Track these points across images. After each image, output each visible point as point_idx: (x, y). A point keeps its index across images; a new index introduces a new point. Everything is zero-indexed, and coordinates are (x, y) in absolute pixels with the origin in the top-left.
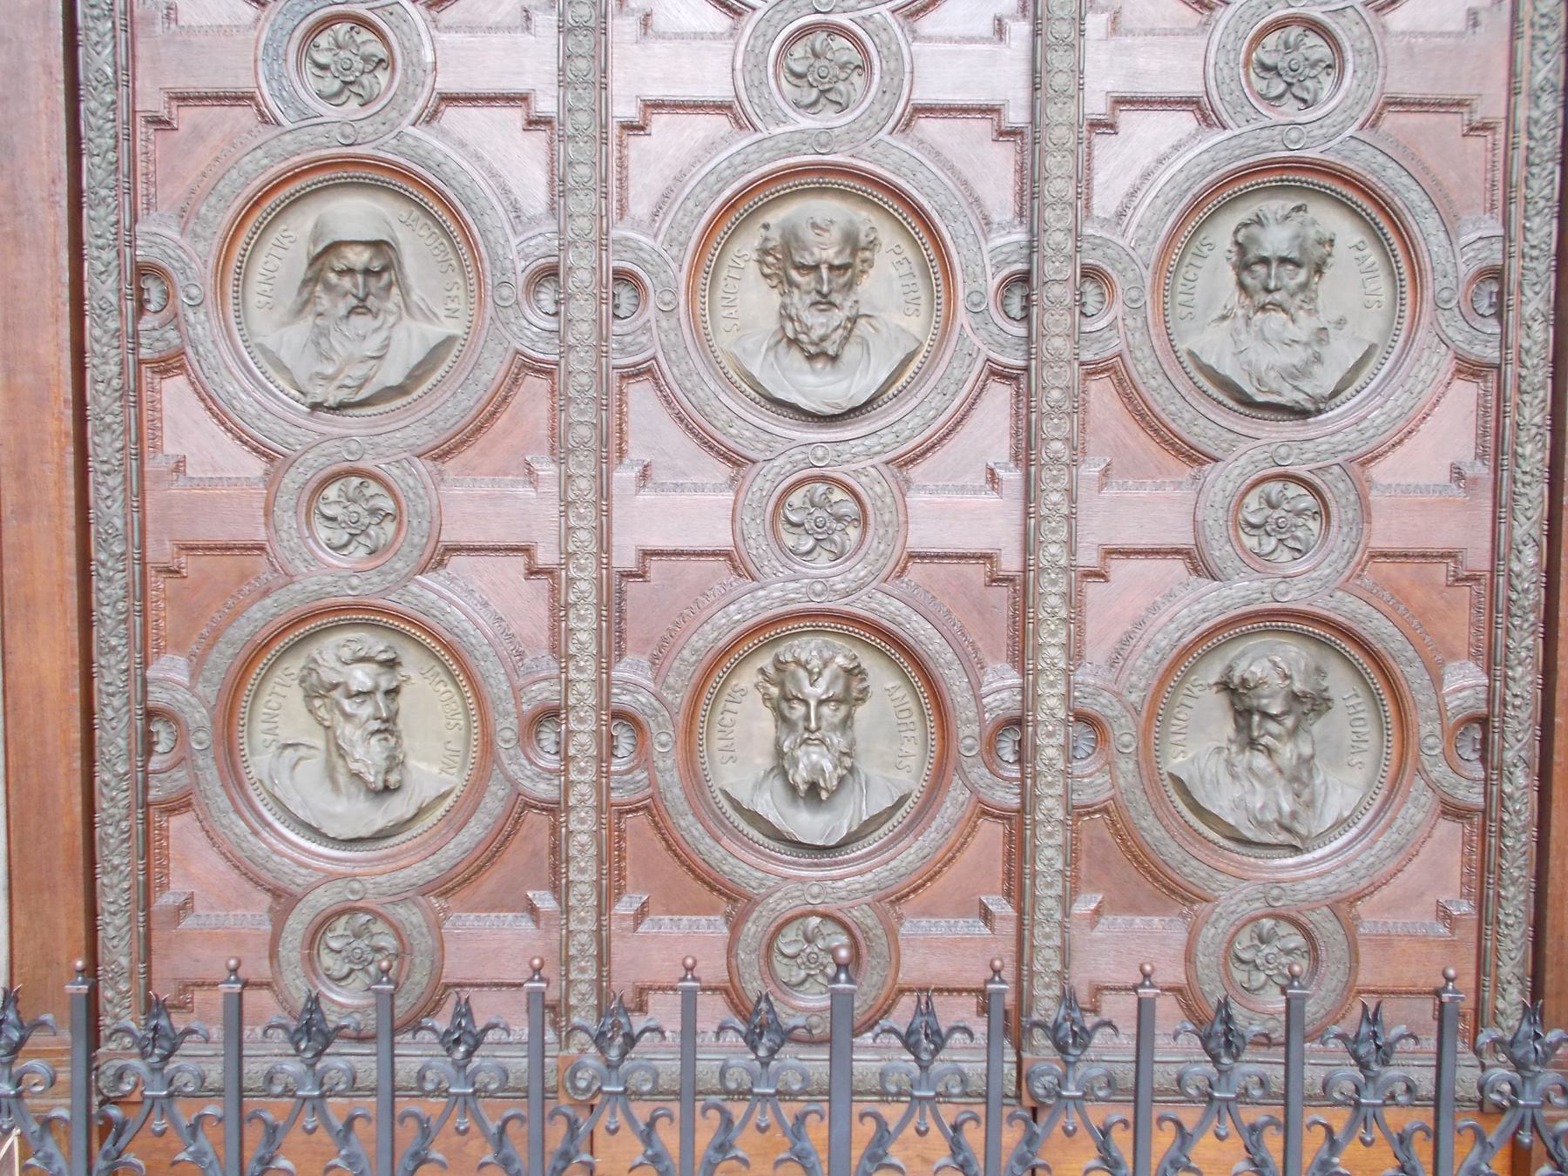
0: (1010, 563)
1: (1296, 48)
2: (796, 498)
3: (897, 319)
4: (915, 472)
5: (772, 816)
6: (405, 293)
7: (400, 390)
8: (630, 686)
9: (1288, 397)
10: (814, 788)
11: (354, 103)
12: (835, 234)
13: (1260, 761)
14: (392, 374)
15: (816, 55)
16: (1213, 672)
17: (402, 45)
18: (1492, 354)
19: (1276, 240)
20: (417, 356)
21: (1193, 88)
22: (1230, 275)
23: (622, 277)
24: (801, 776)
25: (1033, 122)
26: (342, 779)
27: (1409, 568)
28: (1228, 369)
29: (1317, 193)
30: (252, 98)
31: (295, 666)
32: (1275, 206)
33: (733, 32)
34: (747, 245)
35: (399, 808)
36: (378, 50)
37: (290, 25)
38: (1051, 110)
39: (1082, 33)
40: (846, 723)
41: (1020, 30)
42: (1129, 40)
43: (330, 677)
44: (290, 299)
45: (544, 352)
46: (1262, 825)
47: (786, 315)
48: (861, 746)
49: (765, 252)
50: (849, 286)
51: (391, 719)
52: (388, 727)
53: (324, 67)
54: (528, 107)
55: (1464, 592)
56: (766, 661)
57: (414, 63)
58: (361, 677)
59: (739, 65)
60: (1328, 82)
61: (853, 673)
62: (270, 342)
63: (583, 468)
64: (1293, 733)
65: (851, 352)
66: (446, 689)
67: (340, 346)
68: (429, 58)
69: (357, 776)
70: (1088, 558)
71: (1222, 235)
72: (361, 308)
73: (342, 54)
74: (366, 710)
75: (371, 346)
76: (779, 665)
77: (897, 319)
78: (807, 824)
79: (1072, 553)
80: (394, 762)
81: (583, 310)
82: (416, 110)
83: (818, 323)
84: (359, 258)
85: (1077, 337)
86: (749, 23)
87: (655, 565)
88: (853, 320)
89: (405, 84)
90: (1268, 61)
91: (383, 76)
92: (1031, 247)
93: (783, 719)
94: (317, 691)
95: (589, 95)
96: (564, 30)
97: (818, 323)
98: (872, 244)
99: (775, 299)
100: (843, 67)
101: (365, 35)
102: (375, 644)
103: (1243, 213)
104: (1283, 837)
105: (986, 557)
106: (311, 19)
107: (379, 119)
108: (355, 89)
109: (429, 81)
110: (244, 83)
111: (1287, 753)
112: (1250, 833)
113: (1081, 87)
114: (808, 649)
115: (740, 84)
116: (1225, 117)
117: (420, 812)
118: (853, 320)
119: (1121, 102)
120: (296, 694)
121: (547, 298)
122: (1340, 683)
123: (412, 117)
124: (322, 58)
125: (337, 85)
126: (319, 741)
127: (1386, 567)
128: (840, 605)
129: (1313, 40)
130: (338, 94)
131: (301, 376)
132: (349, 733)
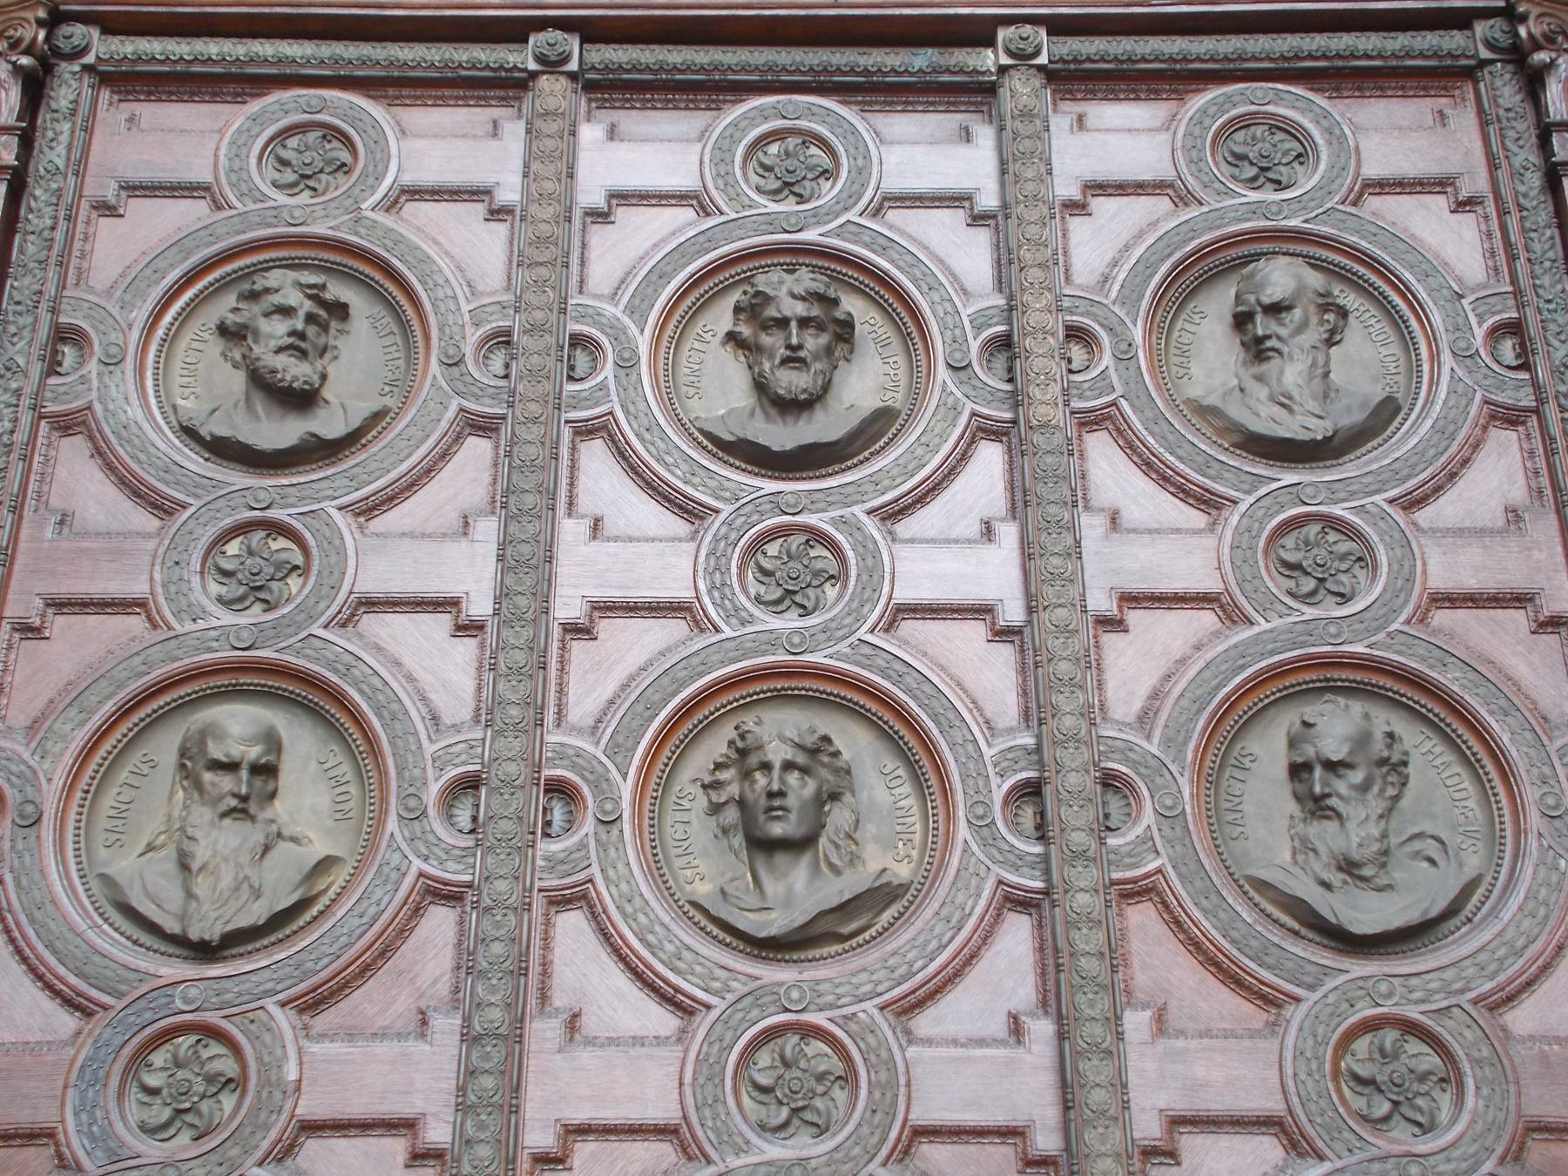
1: (1396, 1056)
11: (185, 1138)
15: (787, 1064)
17: (259, 1059)
25: (1067, 1148)
30: (51, 1134)
33: (682, 1036)
36: (228, 1066)
37: (119, 1040)
38: (1090, 1136)
39: (1120, 1036)
41: (1042, 1029)
42: (1180, 1043)
53: (154, 1092)
54: (415, 1136)
57: (271, 1079)
59: (688, 1078)
60: (1445, 1100)
68: (291, 1073)
73: (180, 1074)
82: (265, 1145)
86: (703, 1024)
89: (255, 1110)
90: (1363, 1071)
91: (228, 1101)
95: (493, 1122)
96: (469, 1038)
100: (820, 1077)
101: (215, 1048)
106: (148, 1031)
107: (214, 1158)
108: (189, 1118)
109: (288, 1106)
110: (44, 1115)
113: (1126, 1105)
115: (690, 1101)
116: (1320, 1144)
119: (1178, 1122)
123: (259, 1154)
124: (152, 1081)
125: (166, 1114)
129: (1414, 1046)
130: (165, 1126)
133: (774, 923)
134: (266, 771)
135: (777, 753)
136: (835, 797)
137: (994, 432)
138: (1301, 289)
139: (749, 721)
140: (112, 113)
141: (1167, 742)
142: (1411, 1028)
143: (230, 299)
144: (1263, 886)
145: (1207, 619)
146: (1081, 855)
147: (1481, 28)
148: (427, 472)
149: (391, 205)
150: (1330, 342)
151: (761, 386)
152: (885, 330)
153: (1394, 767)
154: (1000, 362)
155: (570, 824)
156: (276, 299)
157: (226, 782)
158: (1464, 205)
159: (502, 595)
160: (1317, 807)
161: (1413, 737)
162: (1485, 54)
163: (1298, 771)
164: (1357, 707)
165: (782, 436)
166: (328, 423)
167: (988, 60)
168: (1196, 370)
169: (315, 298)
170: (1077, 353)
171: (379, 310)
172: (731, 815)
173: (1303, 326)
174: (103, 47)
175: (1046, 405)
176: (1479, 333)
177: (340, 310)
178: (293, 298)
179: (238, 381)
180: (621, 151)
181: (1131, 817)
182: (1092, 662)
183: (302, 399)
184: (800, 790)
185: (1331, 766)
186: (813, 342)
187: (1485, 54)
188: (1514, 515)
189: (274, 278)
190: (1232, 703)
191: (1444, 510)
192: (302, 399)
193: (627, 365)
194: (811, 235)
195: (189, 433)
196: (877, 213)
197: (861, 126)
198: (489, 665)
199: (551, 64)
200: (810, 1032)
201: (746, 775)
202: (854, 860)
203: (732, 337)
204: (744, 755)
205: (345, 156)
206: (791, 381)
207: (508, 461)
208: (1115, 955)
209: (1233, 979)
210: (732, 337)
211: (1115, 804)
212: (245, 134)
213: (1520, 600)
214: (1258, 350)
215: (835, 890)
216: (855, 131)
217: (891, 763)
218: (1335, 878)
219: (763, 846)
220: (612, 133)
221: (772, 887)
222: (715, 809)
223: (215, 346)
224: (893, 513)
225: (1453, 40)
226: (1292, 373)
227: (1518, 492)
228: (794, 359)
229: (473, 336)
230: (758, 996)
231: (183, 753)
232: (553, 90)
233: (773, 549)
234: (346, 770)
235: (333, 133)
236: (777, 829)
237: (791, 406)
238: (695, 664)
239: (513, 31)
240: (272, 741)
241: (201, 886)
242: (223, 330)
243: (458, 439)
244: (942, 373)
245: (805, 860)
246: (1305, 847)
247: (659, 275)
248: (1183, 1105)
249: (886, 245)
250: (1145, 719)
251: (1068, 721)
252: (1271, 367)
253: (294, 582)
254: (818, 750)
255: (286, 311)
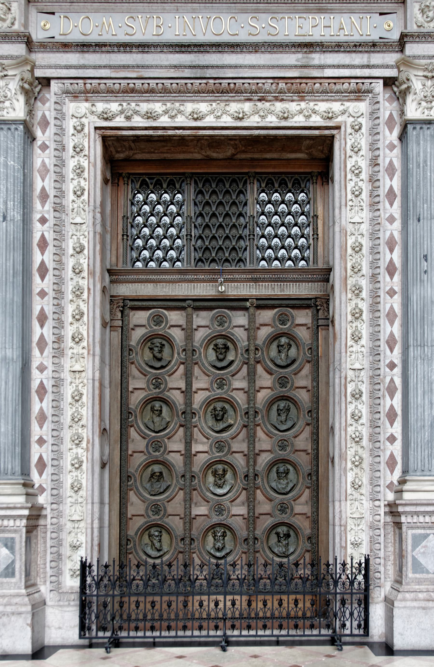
0: (246, 516)
2: (217, 507)
3: (230, 481)
4: (233, 503)
5: (213, 553)
6: (163, 478)
7: (163, 492)
8: (193, 535)
9: (283, 491)
10: (218, 548)
12: (221, 470)
13: (281, 544)
14: (162, 490)
16: (274, 531)
18: (310, 485)
19: (281, 470)
20: (165, 488)
21: (270, 449)
22: (276, 475)
23: (193, 476)
24: (217, 547)
26: (154, 548)
27: (301, 516)
28: (275, 488)
29: (287, 463)
31: (147, 532)
32: (281, 465)
33: (208, 442)
34: (210, 471)
35: (161, 553)
36: (160, 445)
40: (224, 539)
43: (152, 533)
44: (148, 480)
45: (183, 487)
46: (281, 553)
47: (215, 481)
48: (226, 543)
49: (212, 472)
50: (224, 477)
51: (160, 540)
52: (160, 541)
55: (308, 519)
56: (212, 531)
58: (157, 534)
61: (225, 532)
62: (145, 486)
63: (188, 503)
64: (285, 539)
65: (224, 486)
66: (168, 535)
67: (155, 486)
69: (156, 548)
70: (256, 515)
71: (275, 469)
72: (158, 481)
74: (157, 538)
75: (159, 486)
76: (214, 531)
77: (230, 481)
78: (218, 554)
79: (254, 514)
80: (161, 546)
81: (188, 481)
83: (219, 482)
84: (158, 474)
85: (254, 484)
86: (210, 441)
87: (197, 517)
88: (224, 482)
92: (248, 471)
93: (215, 539)
94: (150, 536)
96: (186, 443)
97: (219, 482)
98: (227, 471)
99: (214, 479)
102: (159, 529)
103: (276, 467)
104: (284, 555)
105: (242, 515)
111: (284, 542)
112: (279, 554)
114: (218, 529)
117: (165, 553)
118: (224, 482)
120: (147, 537)
121: (183, 479)
122: (292, 533)
126: (150, 543)
127: (297, 516)
128: (222, 522)
129: (285, 442)
131: (149, 490)
132: (155, 542)
133: (218, 429)
134: (161, 411)
135: (219, 409)
136: (225, 413)
137: (246, 363)
138: (285, 342)
139: (215, 404)
140: (132, 313)
141: (263, 407)
142: (285, 440)
143: (149, 344)
144: (272, 424)
145: (270, 390)
146: (252, 422)
147: (313, 300)
148: (176, 370)
149: (169, 328)
150: (288, 350)
151: (217, 357)
152: (233, 347)
153: (288, 410)
154: (247, 353)
155: (195, 417)
156: (156, 345)
157: (157, 412)
158: (308, 328)
159: (186, 389)
160: (279, 415)
161: (292, 406)
162: (313, 305)
163: (278, 410)
164: (285, 402)
165: (220, 365)
166: (163, 363)
167: (248, 304)
168: (272, 353)
169: (161, 344)
170: (257, 352)
171: (168, 344)
172: (213, 416)
173: (285, 348)
174: (130, 304)
175: (252, 362)
176: (306, 349)
177: (164, 345)
178: (158, 345)
179: (151, 355)
180: (199, 320)
181: (258, 416)
182: (255, 397)
183: (160, 360)
184: (221, 413)
185: (281, 410)
186: (223, 351)
187: (313, 305)
188: (307, 376)
189: (155, 341)
190: (271, 402)
191: (300, 374)
192: (160, 360)
193: (200, 354)
194: (223, 333)
195: (147, 364)
196: (233, 328)
197: (231, 314)
198: (185, 397)
199: (189, 306)
200: (222, 441)
201: (215, 411)
202: (227, 421)
203: (213, 349)
204: (215, 409)
205: (162, 320)
206: (221, 357)
207: (186, 368)
208: (255, 433)
209: (267, 435)
210: (213, 349)
211: (257, 415)
212: (149, 318)
213: (305, 388)
214: (279, 352)
215: (225, 425)
216: (229, 315)
217: (232, 409)
218: (280, 423)
219: (217, 420)
220: (197, 316)
221: (218, 425)
222: (212, 415)
223: (149, 350)
224: (233, 376)
225: (309, 302)
226: (283, 355)
227: (308, 372)
228: (221, 354)
229: (181, 350)
230: (217, 437)
231: (151, 408)
232: (189, 310)
233: (218, 381)
234: (170, 410)
235: (160, 316)
236: (218, 418)
237: (221, 360)
238: (209, 397)
239: (184, 300)
240: (161, 407)
241: (156, 425)
242: (149, 348)
243: (180, 365)
244: (239, 355)
245: (221, 423)
246: (277, 419)
247: (204, 340)
248: (260, 449)
249: (233, 335)
250: (261, 404)
251: (252, 405)
252: (281, 354)
253: (162, 386)
254: (223, 409)
255: (157, 347)
